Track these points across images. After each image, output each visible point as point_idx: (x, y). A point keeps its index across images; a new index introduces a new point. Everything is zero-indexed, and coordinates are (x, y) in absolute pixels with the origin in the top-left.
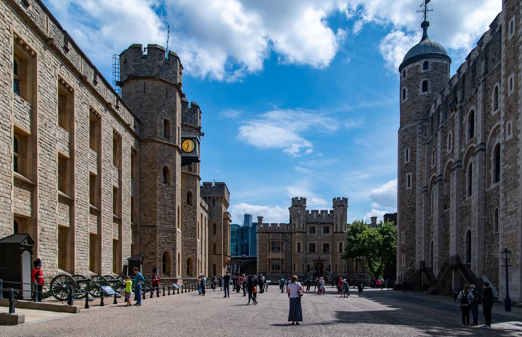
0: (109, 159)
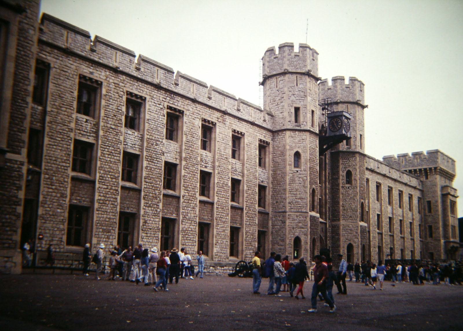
0: (225, 156)
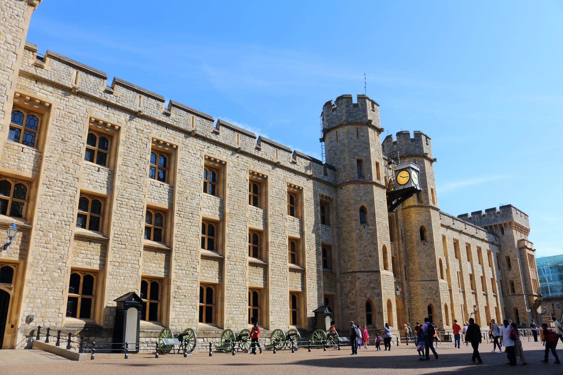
0: (280, 212)
